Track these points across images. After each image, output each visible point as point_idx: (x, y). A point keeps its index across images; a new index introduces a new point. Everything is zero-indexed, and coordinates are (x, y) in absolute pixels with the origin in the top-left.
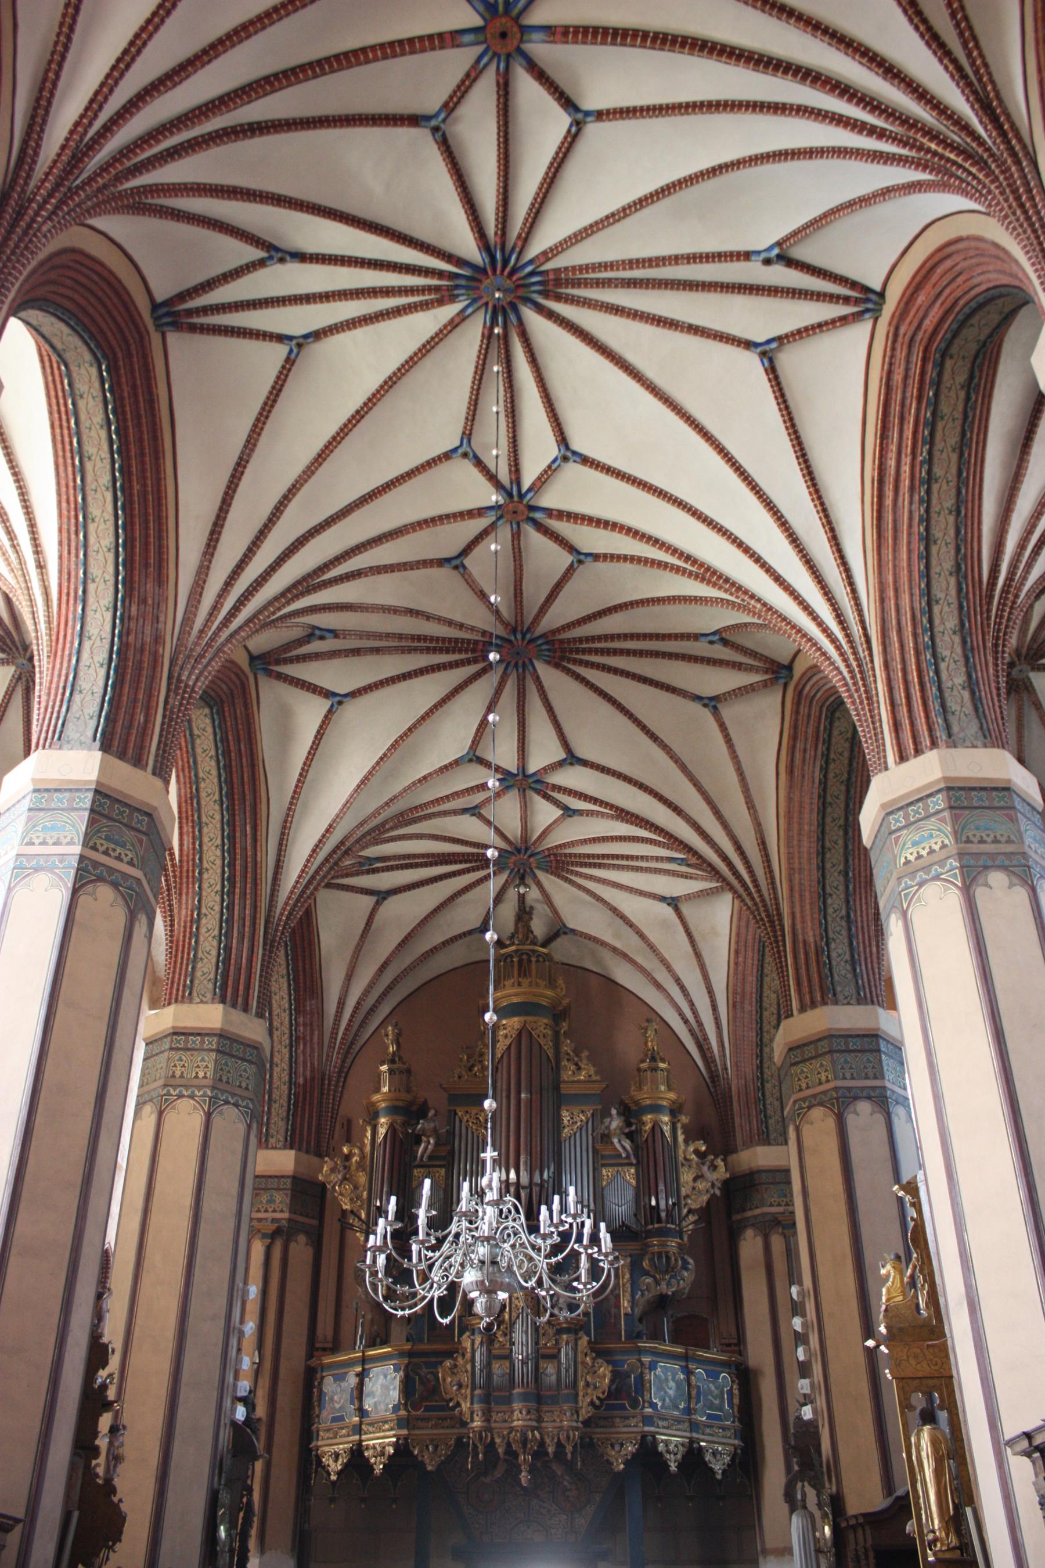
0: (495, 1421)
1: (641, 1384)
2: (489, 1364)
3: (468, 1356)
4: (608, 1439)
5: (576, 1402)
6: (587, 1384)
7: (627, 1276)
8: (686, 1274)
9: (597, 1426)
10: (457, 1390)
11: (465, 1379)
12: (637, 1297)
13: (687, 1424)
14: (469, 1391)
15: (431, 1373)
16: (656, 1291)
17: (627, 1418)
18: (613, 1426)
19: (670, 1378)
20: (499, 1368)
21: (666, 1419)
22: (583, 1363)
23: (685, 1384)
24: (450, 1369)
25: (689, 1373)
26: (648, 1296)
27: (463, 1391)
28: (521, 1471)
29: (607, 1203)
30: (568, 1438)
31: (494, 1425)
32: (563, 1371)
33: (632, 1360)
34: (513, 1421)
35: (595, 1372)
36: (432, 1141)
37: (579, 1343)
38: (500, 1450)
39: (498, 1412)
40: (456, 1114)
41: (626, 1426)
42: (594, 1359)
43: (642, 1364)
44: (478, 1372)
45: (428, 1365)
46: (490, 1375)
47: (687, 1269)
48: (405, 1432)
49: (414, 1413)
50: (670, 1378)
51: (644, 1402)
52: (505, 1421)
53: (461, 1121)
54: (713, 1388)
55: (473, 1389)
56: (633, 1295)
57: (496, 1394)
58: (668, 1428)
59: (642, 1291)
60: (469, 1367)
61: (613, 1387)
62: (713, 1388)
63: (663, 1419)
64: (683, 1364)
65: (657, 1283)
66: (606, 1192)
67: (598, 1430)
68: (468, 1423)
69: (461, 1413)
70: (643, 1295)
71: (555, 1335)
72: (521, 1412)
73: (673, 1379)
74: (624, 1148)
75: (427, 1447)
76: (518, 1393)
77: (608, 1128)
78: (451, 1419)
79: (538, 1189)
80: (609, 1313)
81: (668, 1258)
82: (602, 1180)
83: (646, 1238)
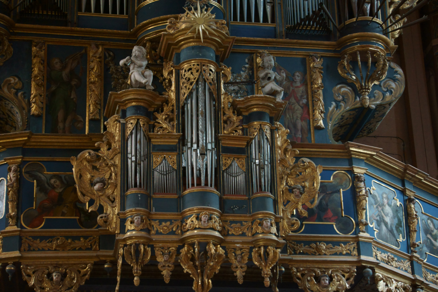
0: (158, 233)
1: (355, 200)
2: (148, 157)
3: (116, 145)
6: (291, 190)
7: (320, 81)
8: (393, 85)
9: (295, 254)
10: (101, 190)
11: (113, 174)
12: (331, 109)
13: (407, 264)
14: (117, 193)
15: (58, 177)
16: (353, 103)
17: (338, 243)
18: (318, 252)
19: (385, 201)
20: (162, 164)
21: (384, 251)
22: (282, 160)
23: (401, 214)
25: (408, 201)
26: (345, 108)
27: (109, 191)
30: (266, 253)
31: (155, 238)
32: (255, 169)
33: (339, 171)
34: (183, 232)
38: (164, 272)
39: (161, 221)
41: (336, 254)
42: (297, 158)
43: (356, 178)
44: (131, 165)
45: (51, 166)
46: (149, 171)
47: (395, 80)
48: (16, 254)
49: (29, 229)
50: (385, 201)
51: (358, 224)
52: (173, 233)
54: (431, 226)
55: (125, 187)
56: (327, 106)
58: (388, 263)
59: (337, 102)
60: (117, 161)
62: (431, 226)
63: (383, 249)
64: (400, 186)
65: (357, 92)
68: (112, 236)
69: (106, 222)
70: (337, 107)
71: (242, 122)
72: (197, 218)
73: (390, 205)
75: (49, 275)
76: (190, 193)
78: (85, 238)
81: (375, 62)
83: (342, 35)
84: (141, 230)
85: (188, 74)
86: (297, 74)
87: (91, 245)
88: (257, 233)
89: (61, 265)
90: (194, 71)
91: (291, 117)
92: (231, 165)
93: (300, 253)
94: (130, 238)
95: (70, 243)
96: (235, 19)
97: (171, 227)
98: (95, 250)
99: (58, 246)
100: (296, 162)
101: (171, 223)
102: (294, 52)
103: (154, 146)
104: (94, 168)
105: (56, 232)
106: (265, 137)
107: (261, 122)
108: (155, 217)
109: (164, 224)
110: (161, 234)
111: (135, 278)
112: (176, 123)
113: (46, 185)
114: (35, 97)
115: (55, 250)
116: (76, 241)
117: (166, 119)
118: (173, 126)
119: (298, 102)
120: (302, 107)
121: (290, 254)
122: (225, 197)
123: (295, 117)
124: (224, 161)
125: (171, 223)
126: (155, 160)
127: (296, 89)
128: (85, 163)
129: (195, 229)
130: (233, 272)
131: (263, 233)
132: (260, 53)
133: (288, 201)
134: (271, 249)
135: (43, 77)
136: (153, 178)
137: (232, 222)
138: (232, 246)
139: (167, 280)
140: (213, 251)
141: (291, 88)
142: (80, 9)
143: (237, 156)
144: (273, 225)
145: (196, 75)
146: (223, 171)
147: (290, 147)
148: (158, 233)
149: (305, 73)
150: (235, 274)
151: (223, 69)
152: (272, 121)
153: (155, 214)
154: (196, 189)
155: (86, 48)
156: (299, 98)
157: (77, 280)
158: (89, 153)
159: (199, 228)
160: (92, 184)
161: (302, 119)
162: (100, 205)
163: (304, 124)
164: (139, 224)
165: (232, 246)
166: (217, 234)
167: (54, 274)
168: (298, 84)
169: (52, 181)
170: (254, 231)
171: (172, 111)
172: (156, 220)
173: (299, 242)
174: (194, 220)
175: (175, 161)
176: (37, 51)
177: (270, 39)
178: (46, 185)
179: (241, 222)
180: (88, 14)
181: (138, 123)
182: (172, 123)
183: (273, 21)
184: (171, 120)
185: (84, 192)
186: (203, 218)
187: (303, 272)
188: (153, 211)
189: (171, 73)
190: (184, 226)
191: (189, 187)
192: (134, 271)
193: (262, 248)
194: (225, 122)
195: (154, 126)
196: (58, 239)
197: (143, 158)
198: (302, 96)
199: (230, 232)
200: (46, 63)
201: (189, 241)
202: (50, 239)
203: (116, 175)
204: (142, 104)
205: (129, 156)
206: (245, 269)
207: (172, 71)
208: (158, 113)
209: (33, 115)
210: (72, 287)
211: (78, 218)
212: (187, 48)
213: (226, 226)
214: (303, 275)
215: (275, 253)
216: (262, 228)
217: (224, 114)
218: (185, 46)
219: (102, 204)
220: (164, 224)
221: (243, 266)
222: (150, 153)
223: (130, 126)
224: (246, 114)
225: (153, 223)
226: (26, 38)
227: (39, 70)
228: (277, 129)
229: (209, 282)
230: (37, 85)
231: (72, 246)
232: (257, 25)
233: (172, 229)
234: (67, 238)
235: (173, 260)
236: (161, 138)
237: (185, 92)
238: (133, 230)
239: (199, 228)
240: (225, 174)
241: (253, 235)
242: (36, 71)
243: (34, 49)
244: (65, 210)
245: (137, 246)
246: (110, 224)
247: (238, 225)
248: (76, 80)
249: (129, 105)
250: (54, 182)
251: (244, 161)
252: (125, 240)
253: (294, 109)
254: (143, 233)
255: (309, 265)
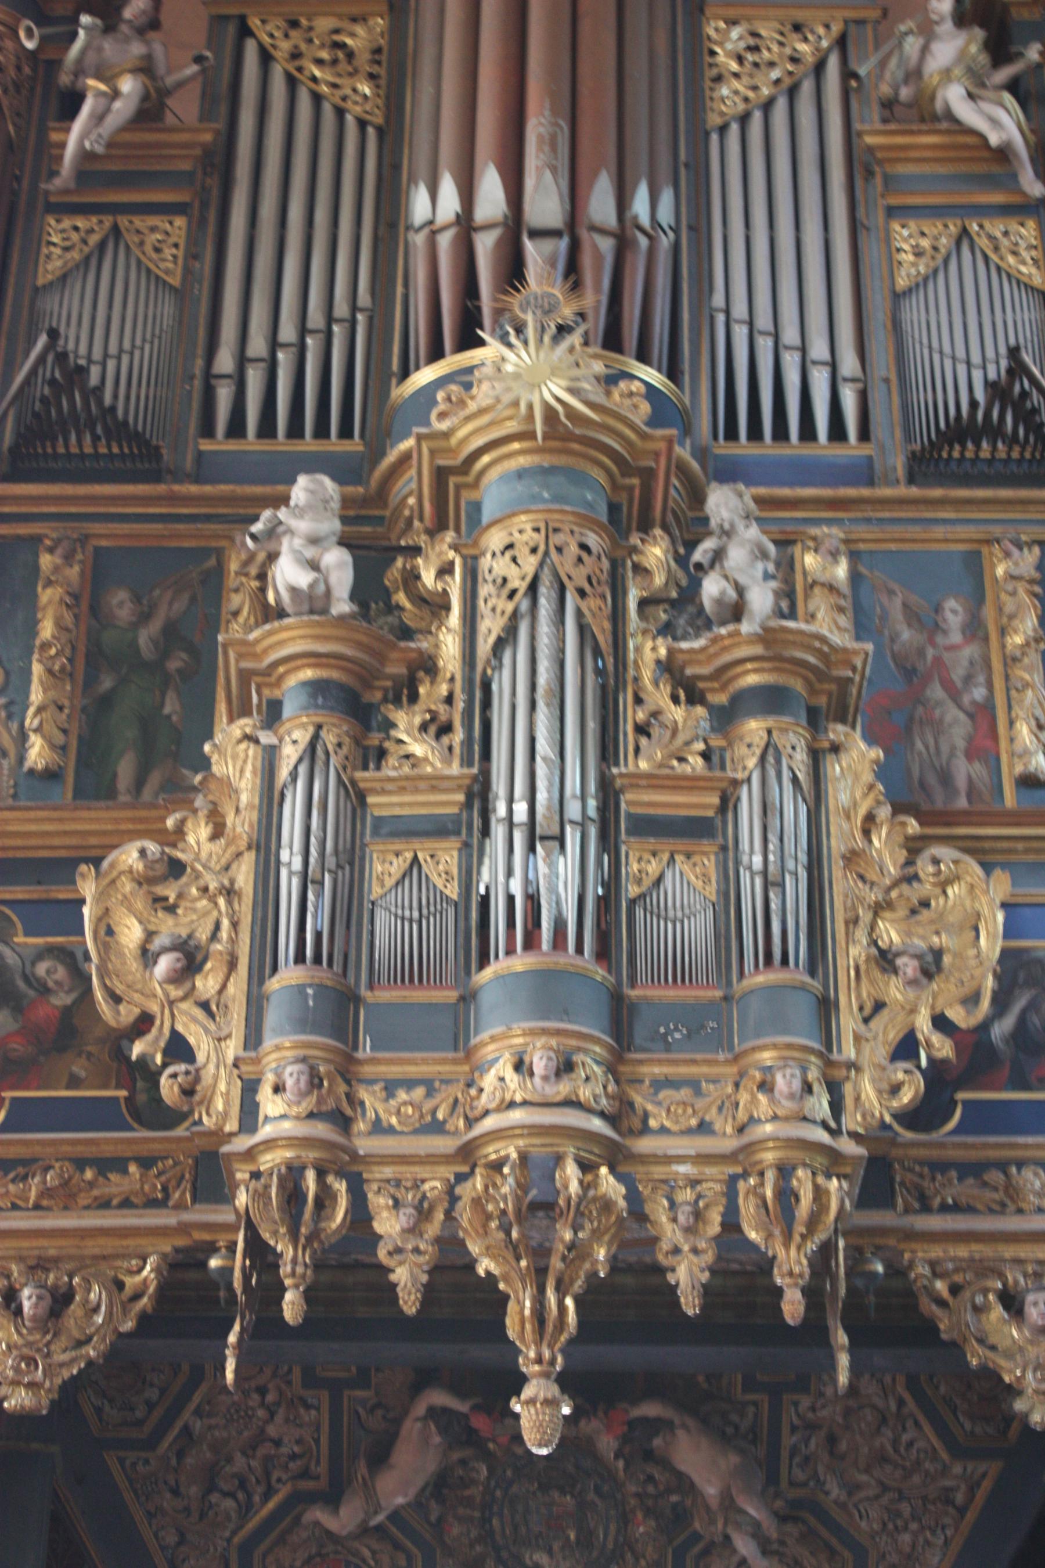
0: (378, 1128)
4: (986, 1269)
5: (828, 1038)
9: (926, 1208)
14: (237, 988)
24: (143, 881)
27: (207, 984)
28: (517, 1382)
29: (918, 353)
30: (786, 1196)
32: (751, 888)
35: (925, 904)
36: (127, 85)
37: (834, 768)
38: (401, 1275)
39: (390, 1088)
40: (245, 32)
42: (914, 847)
44: (289, 886)
52: (437, 1127)
53: (266, 57)
57: (384, 996)
60: (244, 875)
61: (1001, 1029)
66: (913, 313)
67: (935, 1222)
72: (518, 1066)
74: (995, 122)
76: (499, 978)
77: (915, 75)
79: (606, 245)
80: (946, 778)
82: (893, 266)
84: (311, 1115)
85: (502, 566)
86: (951, 604)
87: (165, 1189)
88: (752, 1120)
89: (56, 1261)
90: (522, 552)
91: (932, 750)
92: (659, 881)
93: (944, 1208)
94: (270, 1144)
95: (91, 1184)
96: (732, 434)
97: (427, 1106)
98: (180, 1206)
99: (46, 1192)
100: (909, 863)
101: (430, 1093)
102: (939, 532)
103: (379, 821)
104: (159, 901)
105: (39, 1142)
106: (786, 775)
107: (770, 722)
108: (367, 1070)
109: (402, 1095)
110: (391, 1130)
111: (289, 1296)
112: (458, 736)
113: (21, 984)
114: (40, 710)
115: (37, 1207)
116: (113, 1177)
117: (424, 727)
118: (450, 749)
119: (954, 694)
120: (971, 716)
121: (907, 1210)
122: (633, 993)
123: (945, 749)
124: (635, 867)
125: (430, 1093)
126: (378, 868)
127: (946, 656)
128: (127, 886)
129: (512, 1105)
130: (660, 1271)
131: (775, 1118)
132: (814, 539)
133: (879, 1006)
134: (803, 1181)
135: (73, 648)
136: (372, 933)
137: (659, 1084)
138: (658, 1171)
139: (409, 1303)
140: (574, 1187)
141: (930, 652)
142: (207, 430)
143: (681, 844)
144: (816, 1087)
145: (530, 564)
146: (632, 903)
147: (884, 812)
148: (378, 1128)
149: (978, 597)
150: (671, 1279)
151: (634, 550)
152: (814, 720)
153: (373, 1061)
154: (521, 962)
155: (219, 553)
156: (959, 684)
157: (109, 1314)
158: (143, 852)
159: (525, 1103)
160: (147, 956)
161: (971, 754)
162: (174, 1032)
163: (978, 770)
164: (303, 1095)
165: (658, 1171)
166: (597, 1124)
167: (26, 1292)
168: (956, 638)
169: (41, 969)
170: (742, 1115)
171: (449, 700)
172: (371, 1082)
173: (940, 1167)
174: (510, 1075)
175: (455, 871)
176: (56, 569)
177: (851, 492)
178: (21, 984)
179: (694, 1085)
180: (233, 446)
181: (315, 738)
182: (445, 740)
183: (864, 434)
184: (446, 729)
185: (119, 988)
186: (539, 1064)
187: (958, 1278)
188: (366, 1050)
189: (445, 570)
190: (472, 1099)
191: (497, 956)
192: (285, 1269)
193: (770, 1176)
194: (642, 730)
195: (382, 754)
196: (47, 1169)
197: (331, 862)
198: (968, 679)
199: (653, 1123)
200: (85, 606)
201: (492, 1152)
202: (21, 1170)
203: (235, 925)
204: (335, 675)
205: (284, 855)
206: (709, 1257)
207: (452, 563)
208: (397, 701)
209: (32, 772)
210: (88, 1340)
211: (123, 1093)
212: (504, 478)
213: (638, 1100)
214: (955, 1290)
215: (820, 1194)
216: (772, 1100)
217: (638, 701)
218: (493, 474)
219: (180, 1028)
220: (402, 1095)
221: (702, 1245)
222: (363, 846)
223: (290, 754)
224: (720, 699)
225: (364, 1094)
226: (23, 530)
227: (59, 624)
228: (836, 749)
229: (562, 1308)
230: (50, 671)
231: (96, 1192)
232: (808, 451)
233: (434, 1112)
234: (81, 1164)
235: (434, 1228)
236: (402, 790)
237: (490, 627)
238: (284, 1117)
239: (525, 1103)
240: (639, 913)
241: (741, 1130)
242: (47, 630)
243: (46, 561)
244: (79, 1069)
245: (292, 1174)
246: (208, 1102)
247: (685, 1093)
248: (184, 655)
249: (292, 681)
250: (48, 972)
251: (710, 863)
252: (250, 1155)
253: (941, 720)
254: (321, 1130)
255: (979, 1250)
